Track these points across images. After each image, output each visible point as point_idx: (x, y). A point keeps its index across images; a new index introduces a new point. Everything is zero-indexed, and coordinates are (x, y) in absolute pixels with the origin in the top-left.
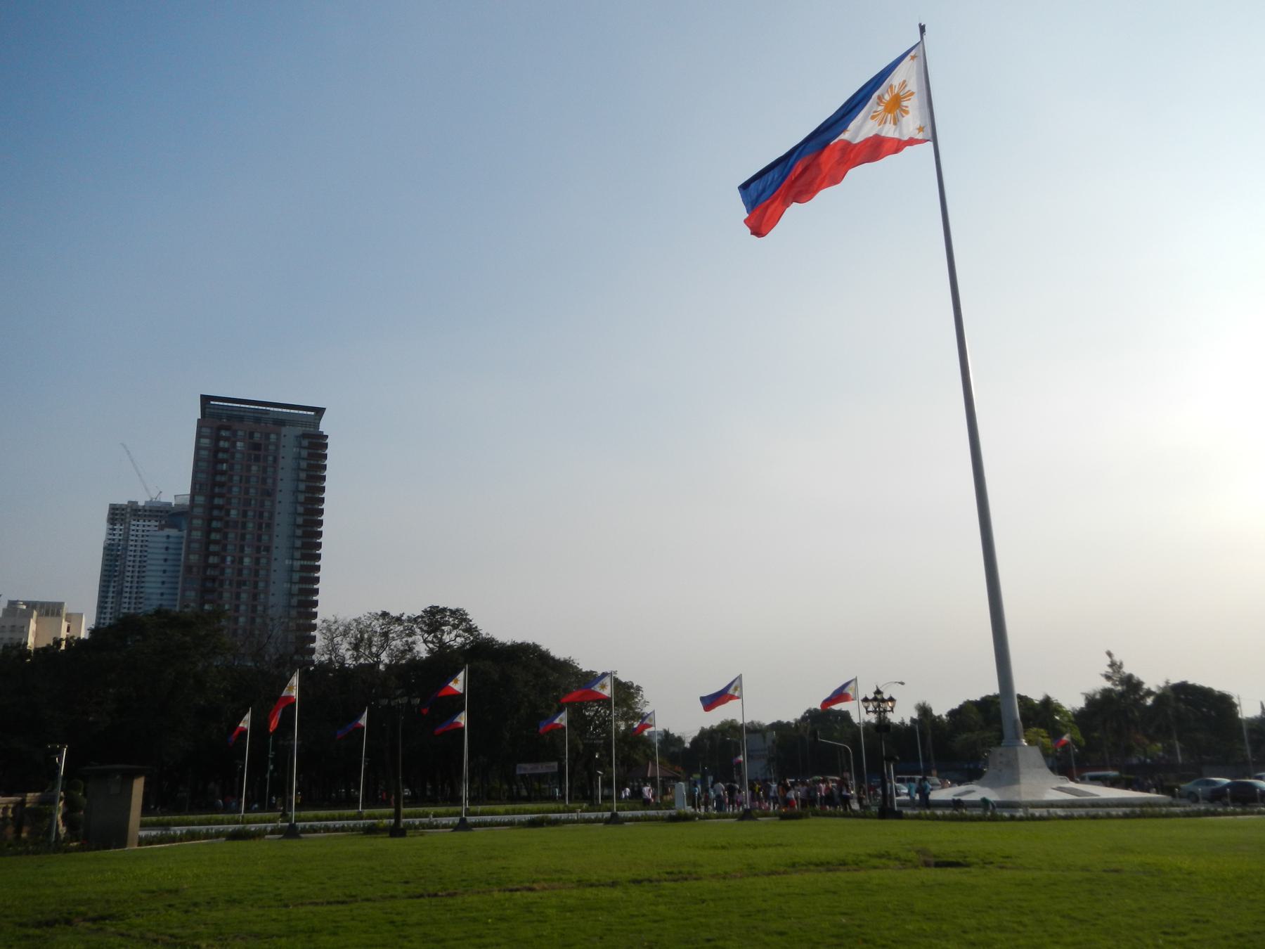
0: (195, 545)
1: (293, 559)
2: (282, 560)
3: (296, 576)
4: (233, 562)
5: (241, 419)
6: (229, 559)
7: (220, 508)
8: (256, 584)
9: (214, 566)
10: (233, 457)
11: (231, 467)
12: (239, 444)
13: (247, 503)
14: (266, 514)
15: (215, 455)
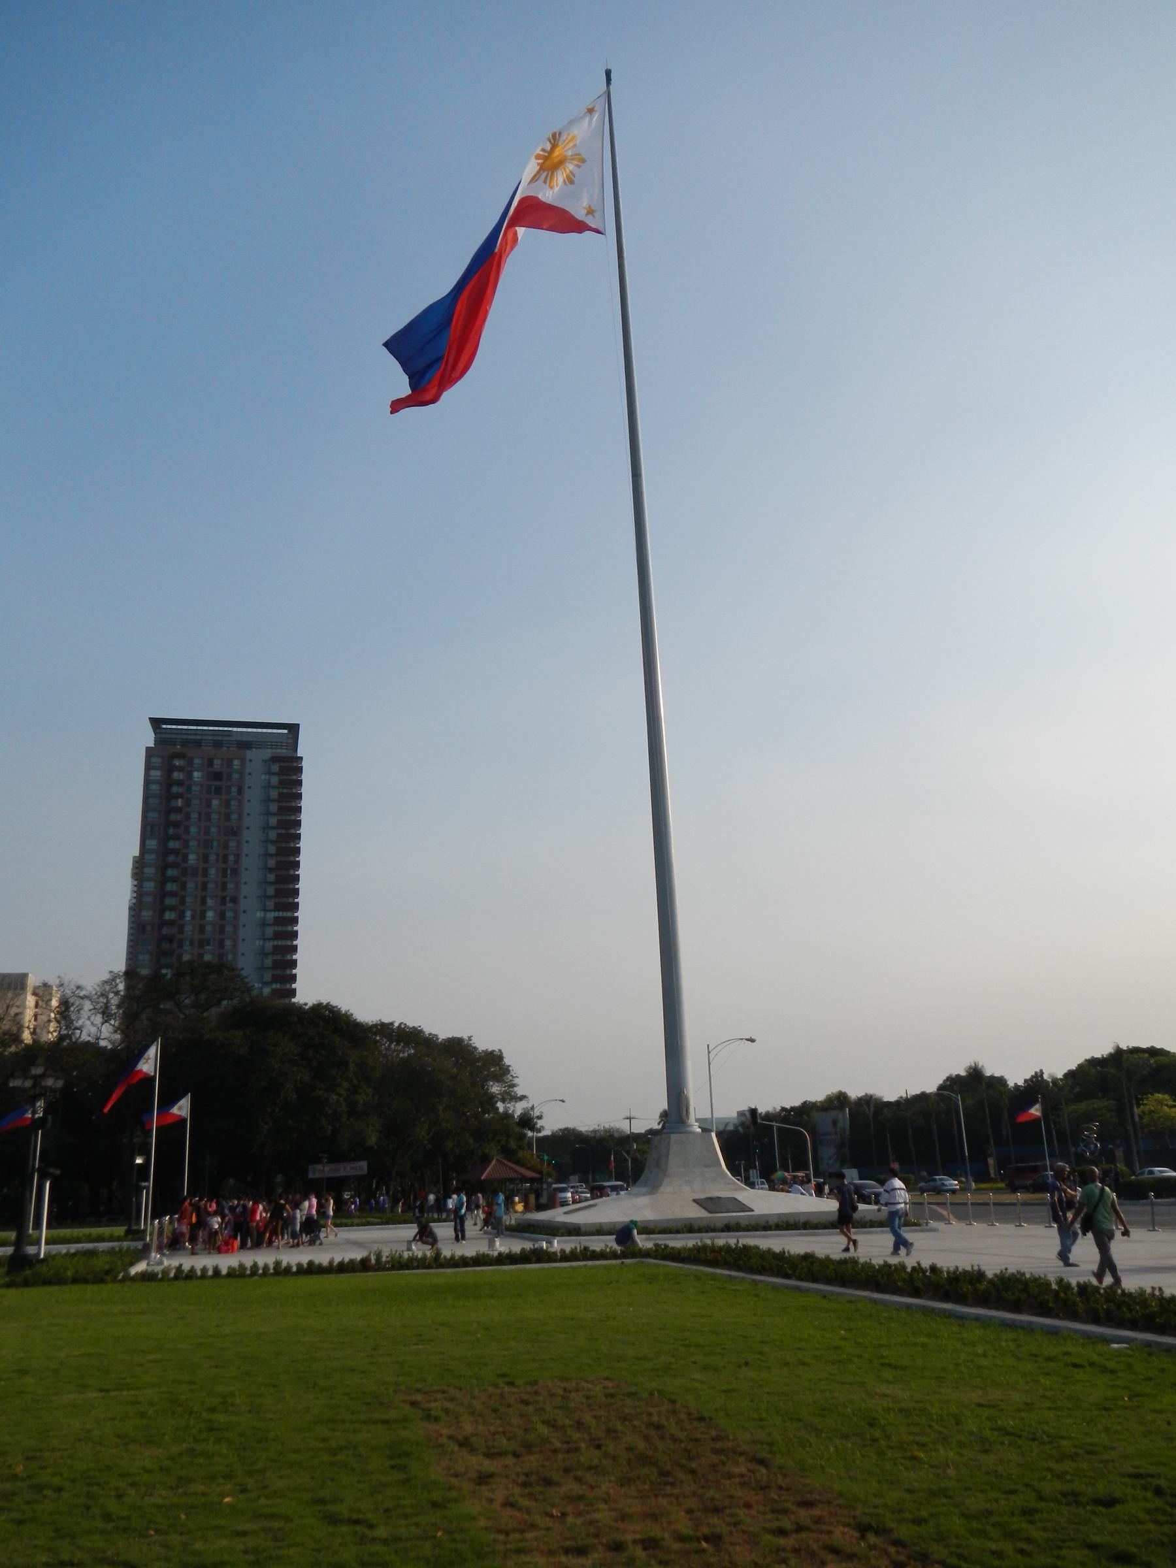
0: (148, 899)
1: (265, 910)
2: (252, 911)
3: (269, 931)
4: (193, 917)
5: (198, 744)
6: (188, 914)
7: (175, 852)
8: (221, 944)
9: (171, 923)
10: (189, 787)
11: (188, 803)
12: (196, 774)
13: (208, 844)
14: (231, 858)
15: (168, 789)
